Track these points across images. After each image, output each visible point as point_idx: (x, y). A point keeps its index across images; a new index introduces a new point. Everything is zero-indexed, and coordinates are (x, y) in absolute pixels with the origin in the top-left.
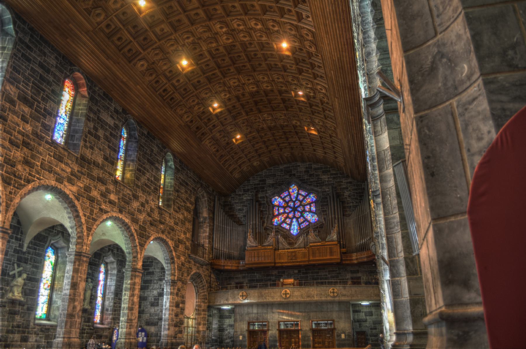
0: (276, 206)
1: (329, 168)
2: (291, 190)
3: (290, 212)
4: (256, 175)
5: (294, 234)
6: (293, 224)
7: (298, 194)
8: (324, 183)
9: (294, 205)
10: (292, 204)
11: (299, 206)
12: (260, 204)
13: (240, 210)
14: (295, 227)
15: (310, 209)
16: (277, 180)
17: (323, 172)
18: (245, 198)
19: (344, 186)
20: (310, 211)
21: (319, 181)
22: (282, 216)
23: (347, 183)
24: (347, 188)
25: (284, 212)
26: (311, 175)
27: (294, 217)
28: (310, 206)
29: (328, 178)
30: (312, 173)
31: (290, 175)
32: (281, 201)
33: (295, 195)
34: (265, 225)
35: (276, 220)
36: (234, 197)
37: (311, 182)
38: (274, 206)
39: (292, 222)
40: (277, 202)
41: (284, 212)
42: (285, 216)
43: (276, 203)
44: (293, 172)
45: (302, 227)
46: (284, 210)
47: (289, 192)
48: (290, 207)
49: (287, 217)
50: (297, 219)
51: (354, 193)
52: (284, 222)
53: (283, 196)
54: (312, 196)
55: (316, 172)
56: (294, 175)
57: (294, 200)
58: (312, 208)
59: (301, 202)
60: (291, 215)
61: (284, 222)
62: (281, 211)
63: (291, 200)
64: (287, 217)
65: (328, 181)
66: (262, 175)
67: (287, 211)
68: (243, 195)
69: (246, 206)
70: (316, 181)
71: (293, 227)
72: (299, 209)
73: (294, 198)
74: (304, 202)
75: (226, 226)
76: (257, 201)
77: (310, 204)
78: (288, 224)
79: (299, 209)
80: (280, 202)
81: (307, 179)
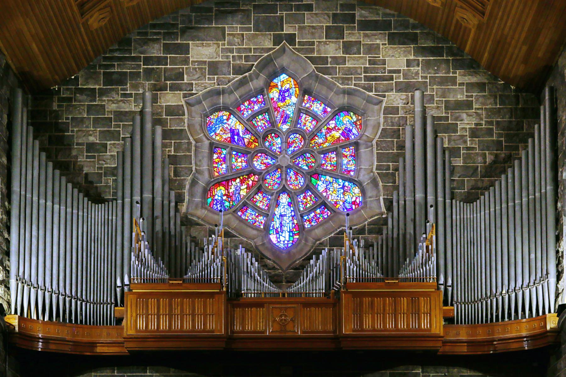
1: (414, 27)
2: (274, 94)
4: (154, 26)
5: (281, 245)
6: (278, 211)
8: (391, 78)
11: (301, 154)
12: (166, 134)
13: (91, 147)
14: (287, 220)
16: (231, 51)
17: (393, 39)
18: (113, 107)
19: (460, 97)
22: (242, 182)
23: (470, 86)
24: (468, 105)
26: (348, 47)
29: (409, 63)
30: (353, 39)
31: (277, 40)
32: (240, 128)
33: (290, 111)
34: (183, 208)
35: (220, 191)
36: (69, 100)
37: (350, 71)
40: (224, 130)
42: (250, 183)
44: (287, 30)
45: (307, 225)
46: (249, 163)
51: (491, 123)
54: (346, 120)
55: (366, 36)
56: (291, 39)
57: (285, 127)
58: (345, 161)
62: (239, 163)
65: (405, 76)
66: (174, 26)
67: (258, 164)
68: (102, 93)
70: (366, 70)
71: (276, 224)
73: (284, 122)
75: (49, 204)
77: (337, 148)
78: (260, 212)
80: (233, 132)
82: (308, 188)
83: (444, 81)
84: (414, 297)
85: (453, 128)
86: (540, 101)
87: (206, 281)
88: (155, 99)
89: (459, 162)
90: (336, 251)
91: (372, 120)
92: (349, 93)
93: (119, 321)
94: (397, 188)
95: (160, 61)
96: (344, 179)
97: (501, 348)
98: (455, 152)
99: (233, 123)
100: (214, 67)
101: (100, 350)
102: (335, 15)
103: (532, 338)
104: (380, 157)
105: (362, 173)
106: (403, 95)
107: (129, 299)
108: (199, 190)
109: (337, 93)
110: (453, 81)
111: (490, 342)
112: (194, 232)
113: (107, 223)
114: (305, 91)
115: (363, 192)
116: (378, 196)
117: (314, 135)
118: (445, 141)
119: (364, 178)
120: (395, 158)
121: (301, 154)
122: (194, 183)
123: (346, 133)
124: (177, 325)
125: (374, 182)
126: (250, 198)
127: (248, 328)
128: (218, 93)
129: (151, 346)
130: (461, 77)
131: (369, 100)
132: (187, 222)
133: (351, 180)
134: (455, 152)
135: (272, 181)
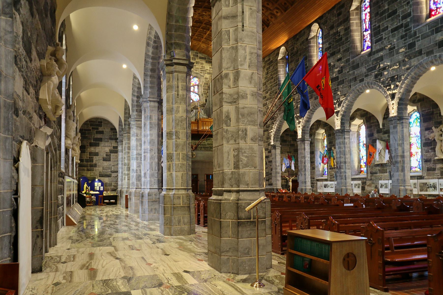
15: (194, 90)
17: (206, 62)
21: (203, 69)
28: (194, 88)
29: (210, 68)
30: (198, 61)
37: (197, 68)
70: (201, 69)
77: (194, 86)
91: (202, 80)
92: (197, 73)
94: (208, 97)
96: (195, 93)
102: (194, 55)
104: (204, 89)
105: (199, 92)
106: (209, 75)
109: (194, 73)
115: (199, 97)
116: (203, 98)
119: (200, 93)
120: (207, 90)
125: (202, 95)
131: (201, 75)
133: (197, 94)
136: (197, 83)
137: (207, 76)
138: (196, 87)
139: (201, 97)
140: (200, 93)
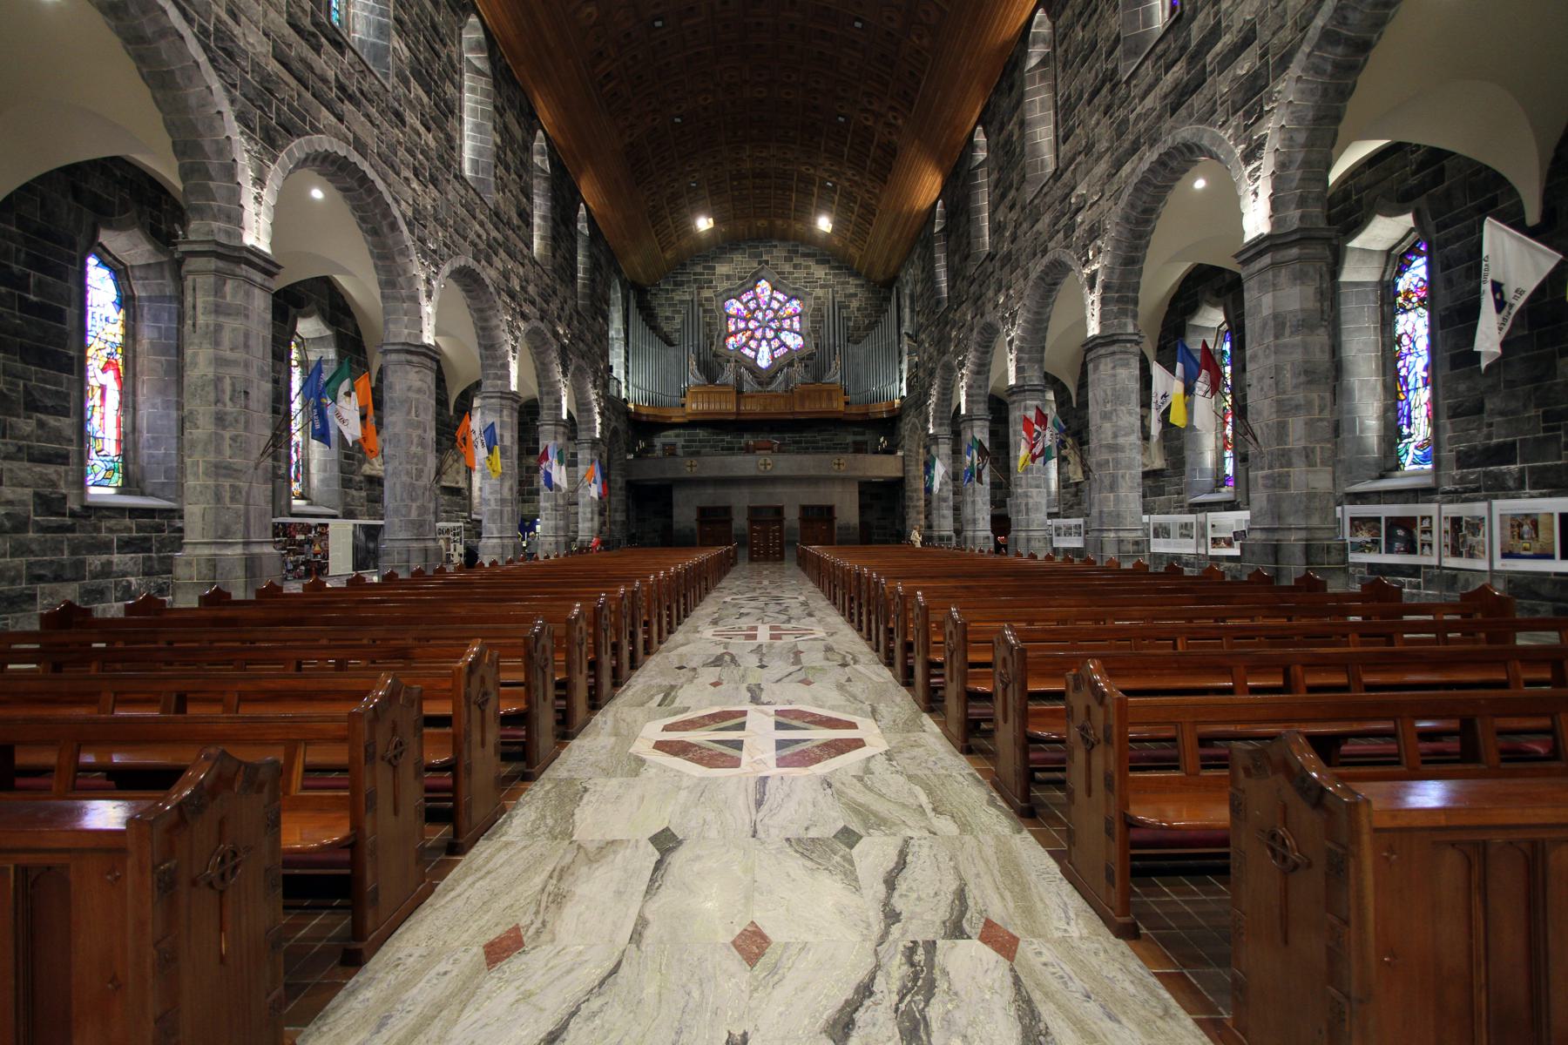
0: (732, 316)
2: (758, 290)
3: (757, 329)
7: (772, 298)
9: (765, 315)
10: (760, 315)
11: (772, 320)
12: (705, 311)
13: (667, 318)
15: (791, 325)
18: (678, 298)
20: (791, 330)
23: (857, 285)
25: (747, 329)
26: (795, 267)
27: (764, 338)
32: (741, 307)
33: (766, 299)
35: (731, 340)
38: (729, 317)
39: (759, 345)
41: (747, 329)
43: (732, 311)
44: (765, 258)
47: (755, 293)
48: (756, 319)
49: (752, 338)
50: (769, 341)
52: (746, 345)
53: (745, 298)
54: (795, 303)
59: (776, 311)
60: (758, 334)
61: (746, 345)
62: (742, 325)
63: (758, 308)
64: (752, 338)
68: (673, 291)
69: (679, 312)
71: (760, 355)
72: (773, 325)
74: (781, 313)
76: (700, 305)
77: (790, 317)
79: (773, 325)
81: (789, 273)
82: (776, 337)
83: (843, 283)
84: (830, 393)
85: (848, 307)
86: (891, 292)
87: (726, 385)
88: (699, 294)
89: (851, 324)
90: (791, 369)
92: (796, 289)
93: (683, 405)
95: (702, 274)
97: (873, 417)
98: (849, 319)
99: (738, 305)
100: (728, 277)
101: (674, 420)
103: (888, 412)
107: (688, 395)
108: (721, 339)
110: (848, 283)
111: (867, 414)
112: (719, 360)
113: (676, 356)
114: (774, 288)
117: (778, 310)
118: (845, 313)
119: (805, 333)
120: (819, 322)
121: (772, 320)
122: (719, 336)
123: (795, 310)
124: (712, 407)
125: (809, 335)
126: (747, 342)
127: (748, 408)
128: (730, 290)
129: (699, 418)
130: (851, 280)
131: (807, 293)
132: (716, 355)
134: (849, 319)
135: (758, 334)
136: (799, 310)
137: (819, 292)
138: (796, 319)
139: (807, 339)
140: (805, 333)
